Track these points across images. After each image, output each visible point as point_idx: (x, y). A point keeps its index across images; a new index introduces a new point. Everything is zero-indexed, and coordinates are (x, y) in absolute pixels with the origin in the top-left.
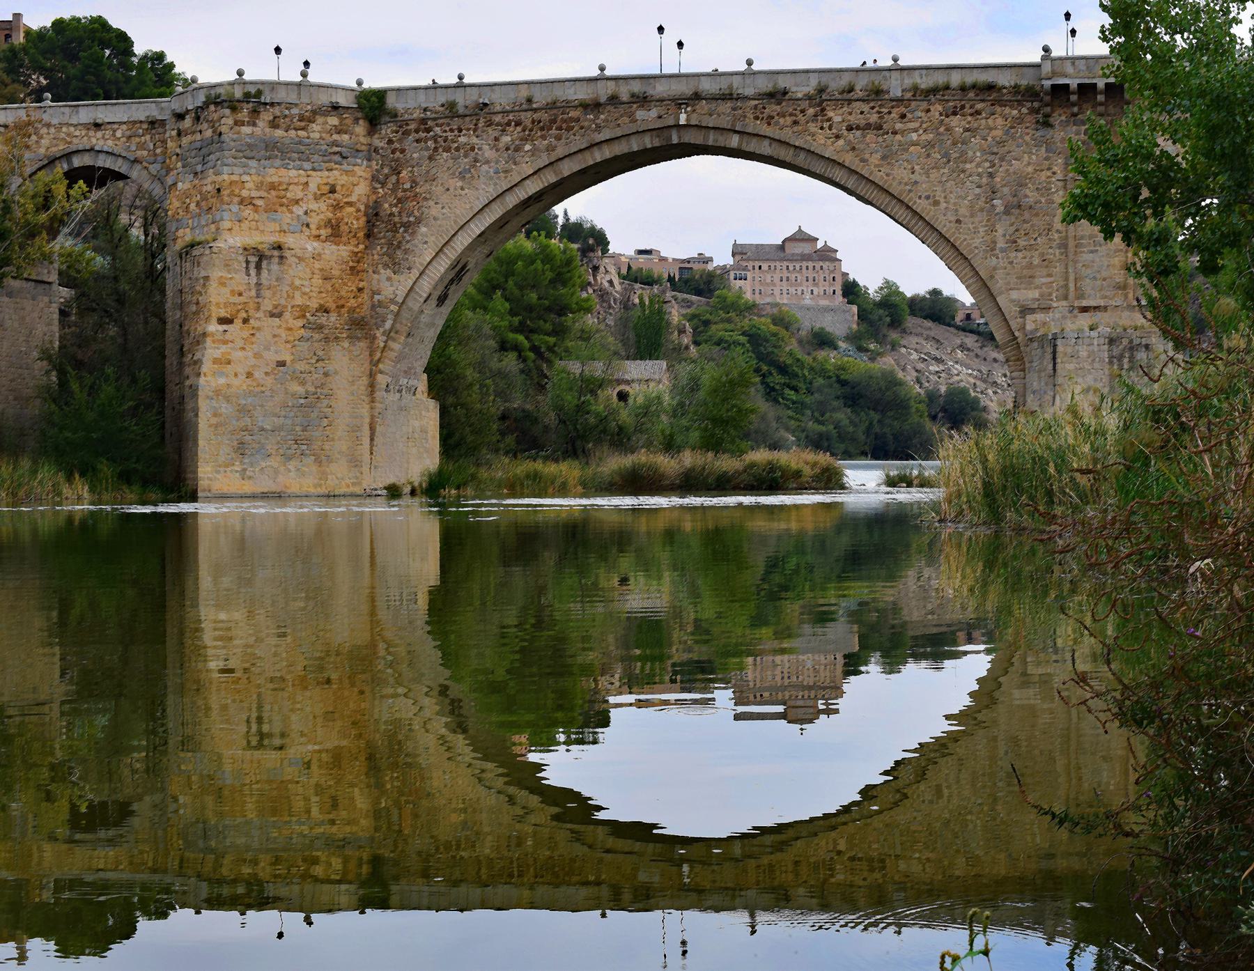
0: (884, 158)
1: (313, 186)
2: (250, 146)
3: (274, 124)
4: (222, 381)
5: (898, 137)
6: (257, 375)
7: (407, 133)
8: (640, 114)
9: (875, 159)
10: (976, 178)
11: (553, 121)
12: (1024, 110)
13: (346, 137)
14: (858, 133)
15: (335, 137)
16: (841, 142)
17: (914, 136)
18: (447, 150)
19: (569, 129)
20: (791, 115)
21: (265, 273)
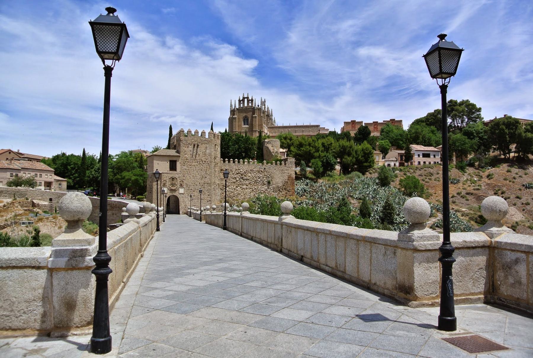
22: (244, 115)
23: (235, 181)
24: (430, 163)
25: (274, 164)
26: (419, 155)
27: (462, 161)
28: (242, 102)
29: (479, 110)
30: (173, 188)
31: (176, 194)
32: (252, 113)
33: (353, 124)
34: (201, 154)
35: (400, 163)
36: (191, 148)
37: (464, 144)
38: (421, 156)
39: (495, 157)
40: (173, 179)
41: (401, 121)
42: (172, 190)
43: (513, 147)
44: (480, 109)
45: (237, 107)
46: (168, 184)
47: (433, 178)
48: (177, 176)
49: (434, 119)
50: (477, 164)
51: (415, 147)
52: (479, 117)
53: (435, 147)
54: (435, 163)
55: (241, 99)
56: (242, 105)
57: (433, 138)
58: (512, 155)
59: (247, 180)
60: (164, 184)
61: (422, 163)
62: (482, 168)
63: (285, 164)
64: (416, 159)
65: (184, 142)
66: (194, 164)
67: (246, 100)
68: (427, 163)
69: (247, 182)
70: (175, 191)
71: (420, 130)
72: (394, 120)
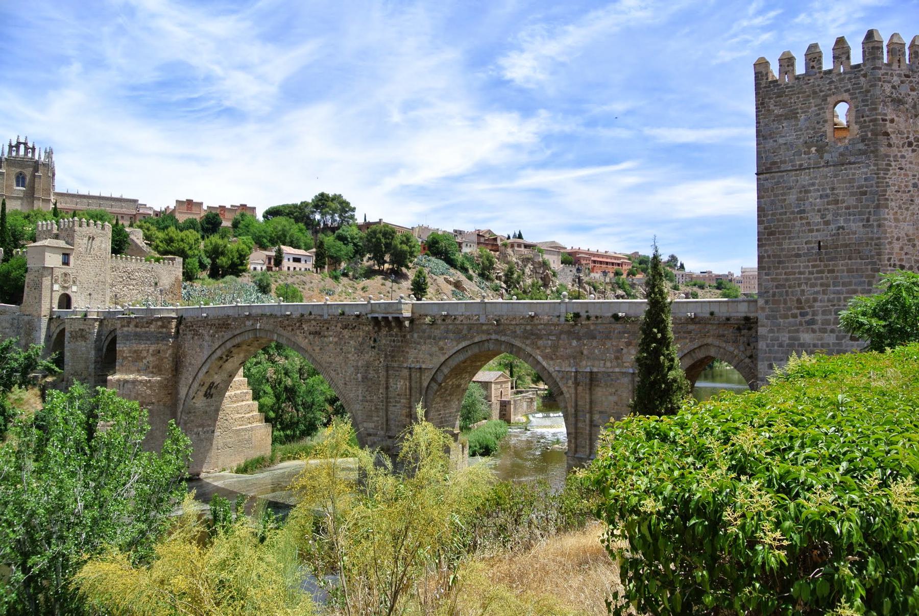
1: (150, 351)
2: (128, 335)
3: (136, 326)
9: (317, 349)
11: (224, 324)
13: (164, 330)
14: (312, 336)
15: (160, 330)
16: (307, 340)
22: (18, 170)
23: (121, 280)
24: (300, 269)
25: (162, 263)
26: (289, 259)
27: (335, 270)
29: (353, 210)
30: (66, 285)
31: (68, 292)
32: (31, 169)
33: (189, 204)
34: (96, 249)
35: (267, 267)
36: (85, 240)
37: (340, 251)
38: (291, 260)
39: (369, 267)
40: (66, 275)
41: (254, 208)
42: (64, 287)
43: (387, 258)
44: (355, 208)
45: (6, 156)
46: (60, 280)
47: (307, 287)
49: (300, 213)
50: (351, 274)
51: (286, 249)
52: (352, 217)
53: (306, 250)
54: (306, 269)
55: (14, 143)
56: (14, 154)
57: (303, 238)
58: (387, 266)
59: (134, 279)
60: (56, 280)
61: (292, 269)
62: (357, 279)
63: (173, 264)
64: (286, 263)
65: (79, 233)
66: (88, 259)
67: (22, 147)
68: (298, 269)
69: (134, 282)
70: (67, 288)
71: (288, 227)
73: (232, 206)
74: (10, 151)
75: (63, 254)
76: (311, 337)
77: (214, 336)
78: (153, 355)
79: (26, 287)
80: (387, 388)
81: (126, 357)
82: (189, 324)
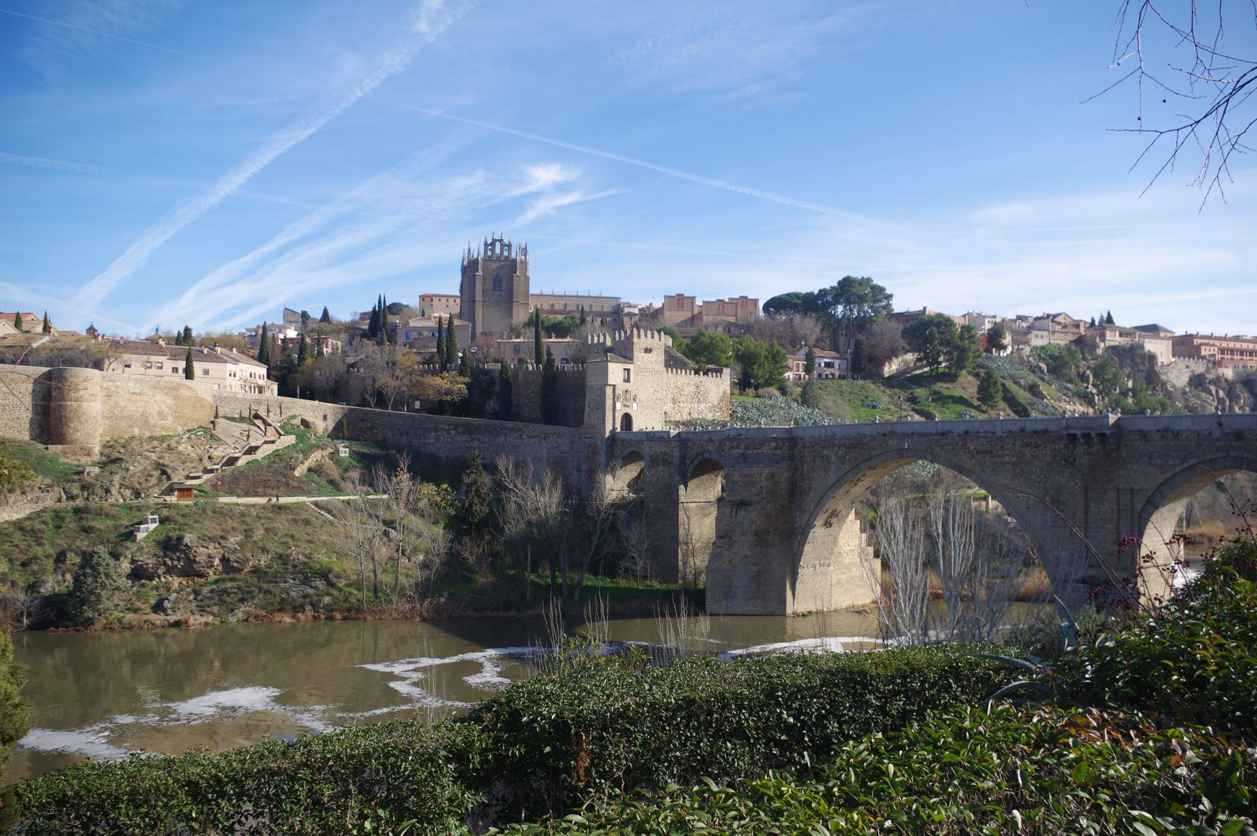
0: (993, 470)
1: (764, 475)
4: (717, 564)
5: (1000, 459)
6: (734, 562)
7: (805, 448)
8: (890, 442)
10: (1037, 484)
12: (1062, 446)
13: (779, 451)
14: (981, 456)
16: (974, 461)
17: (1007, 459)
18: (819, 457)
19: (863, 448)
20: (952, 445)
21: (739, 515)
28: (490, 247)
29: (889, 297)
45: (482, 255)
48: (630, 389)
52: (888, 307)
55: (489, 241)
56: (489, 253)
67: (498, 244)
72: (746, 297)
73: (729, 299)
74: (486, 252)
75: (625, 369)
76: (980, 457)
77: (844, 457)
78: (766, 479)
79: (586, 408)
80: (1086, 512)
81: (737, 482)
82: (808, 445)
